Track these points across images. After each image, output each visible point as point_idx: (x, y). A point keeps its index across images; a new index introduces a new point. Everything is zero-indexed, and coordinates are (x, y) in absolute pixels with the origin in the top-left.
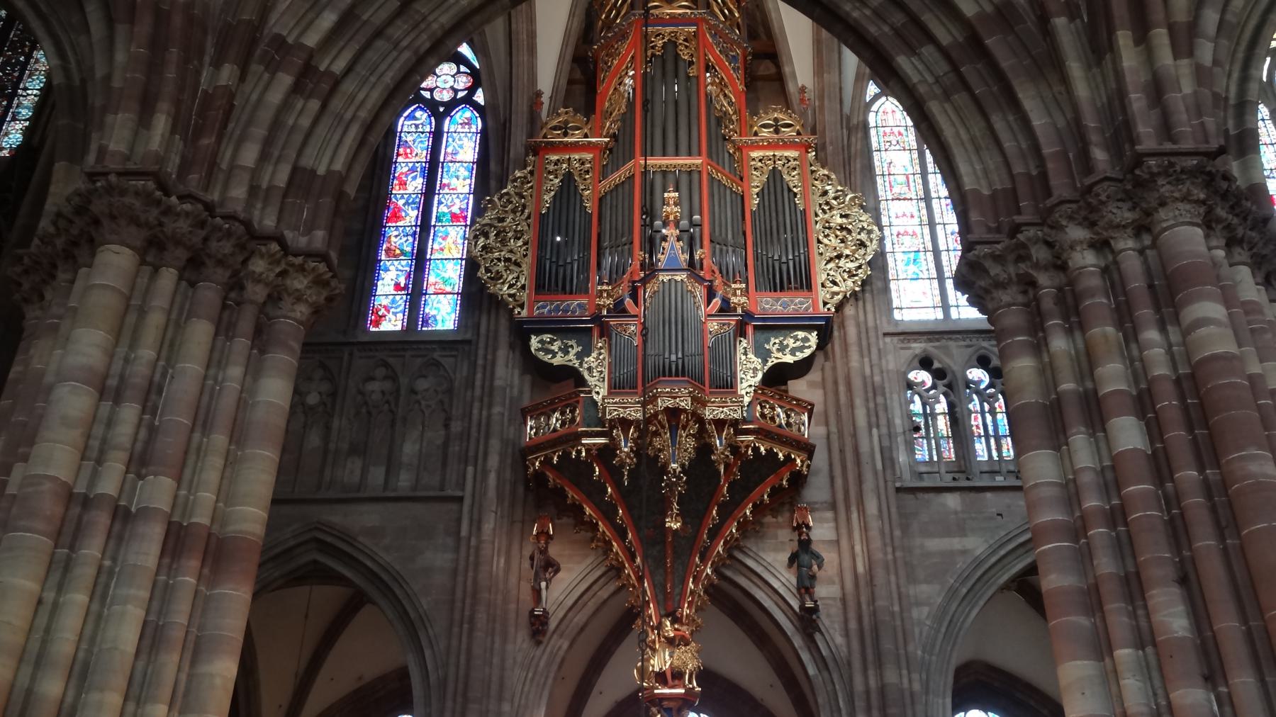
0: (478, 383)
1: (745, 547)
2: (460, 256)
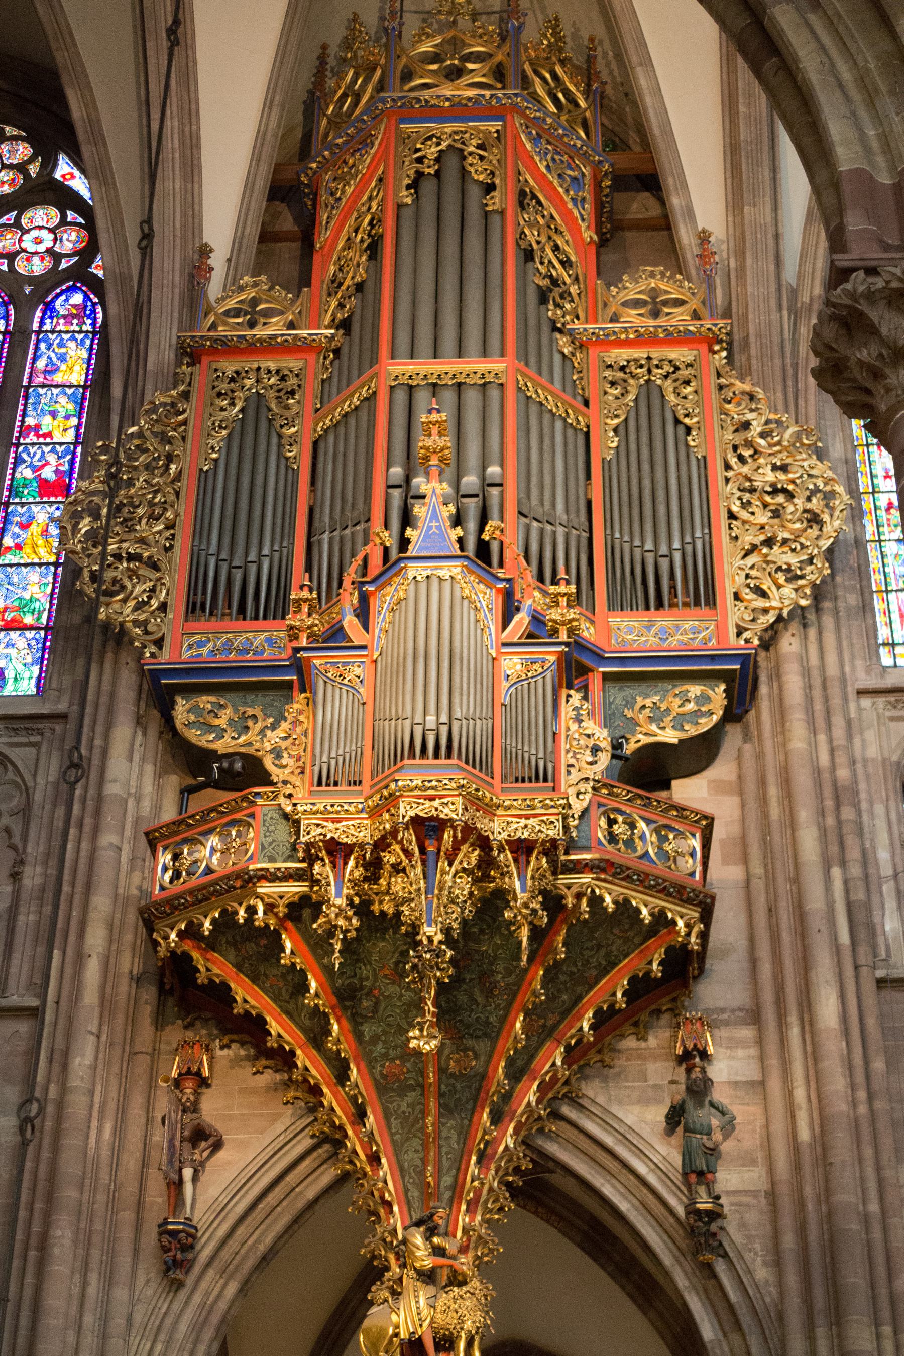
2: (53, 559)
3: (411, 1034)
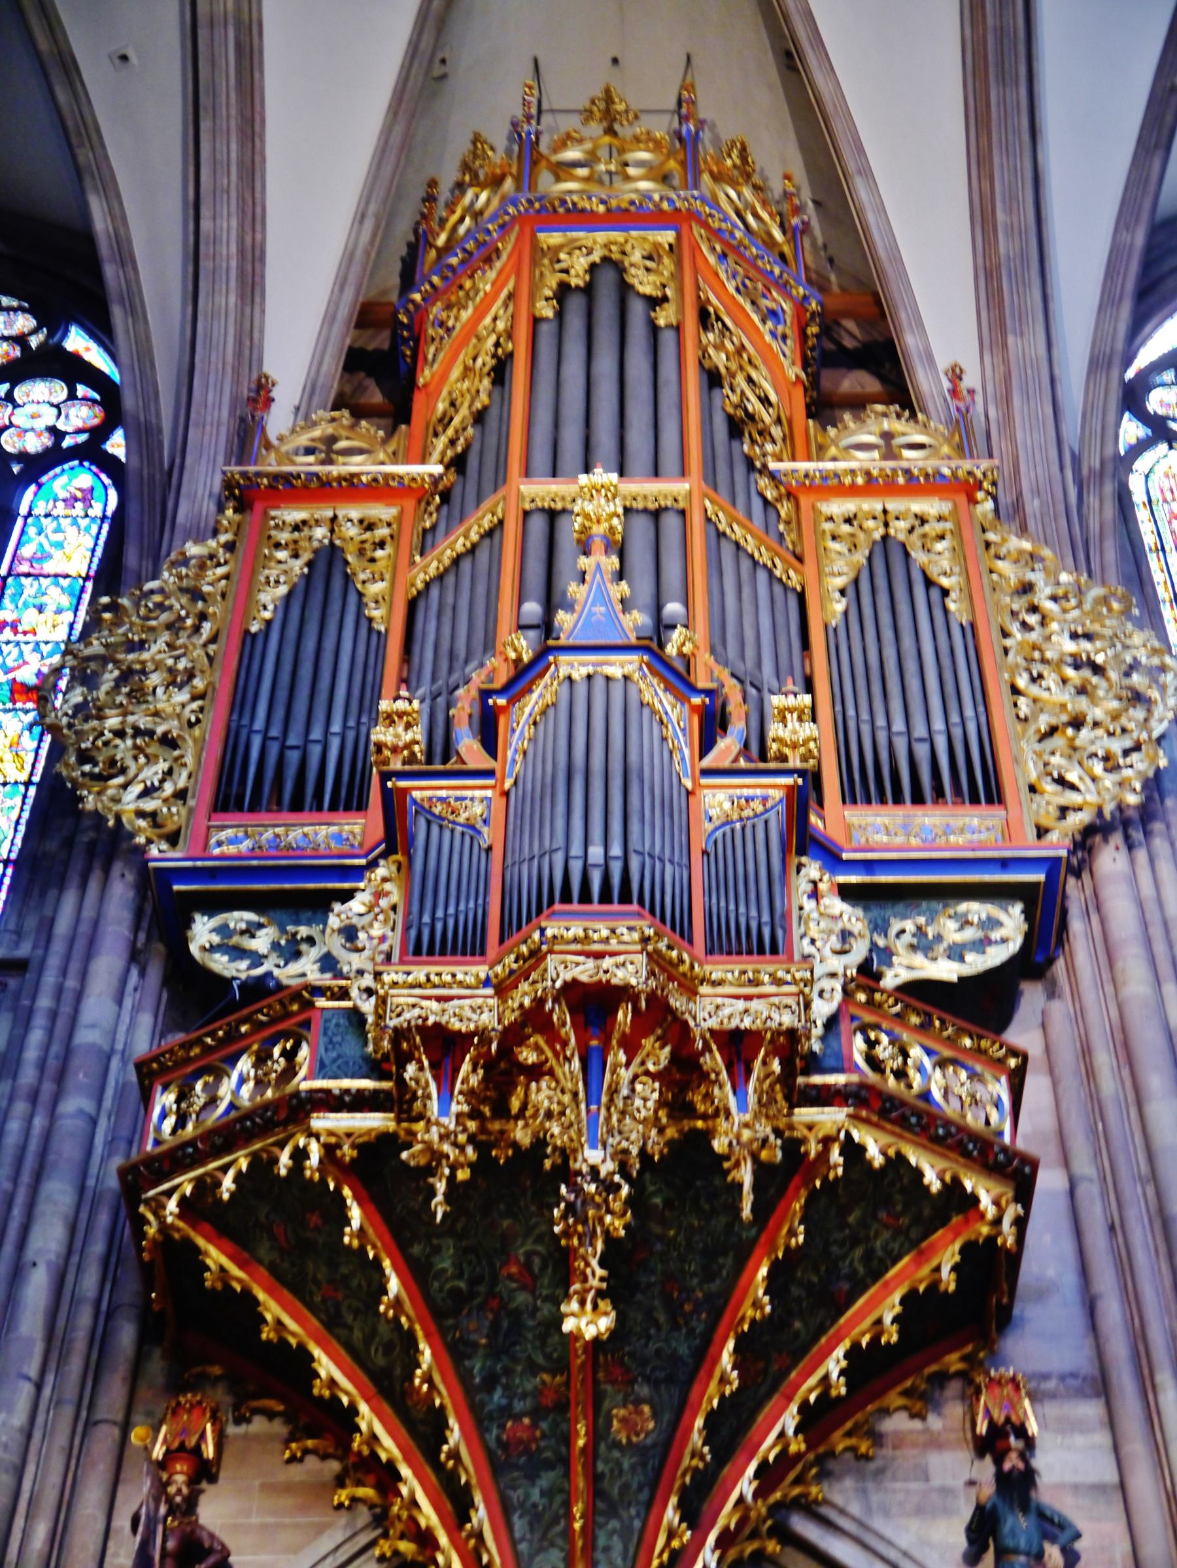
0: (31, 1054)
1: (826, 1502)
3: (564, 1308)
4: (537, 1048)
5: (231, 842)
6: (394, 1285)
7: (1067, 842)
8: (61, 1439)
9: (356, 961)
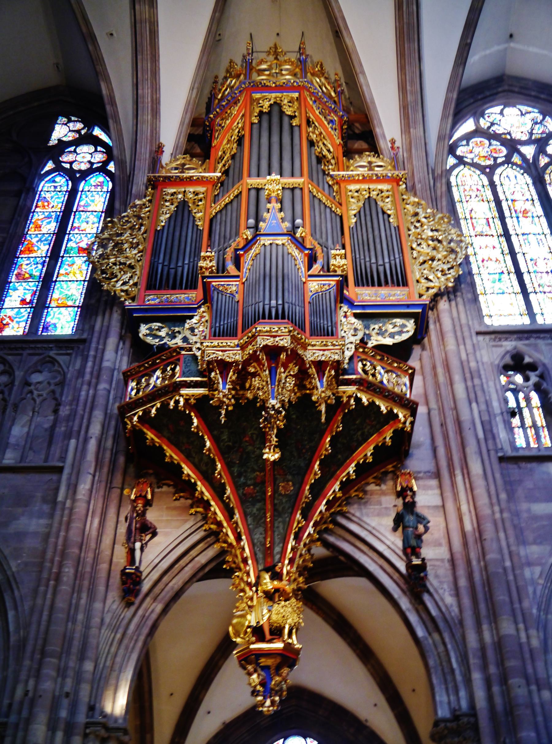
0: (88, 370)
1: (348, 512)
2: (83, 279)
3: (264, 451)
4: (254, 367)
5: (153, 300)
6: (208, 444)
7: (429, 299)
8: (102, 493)
9: (195, 339)
